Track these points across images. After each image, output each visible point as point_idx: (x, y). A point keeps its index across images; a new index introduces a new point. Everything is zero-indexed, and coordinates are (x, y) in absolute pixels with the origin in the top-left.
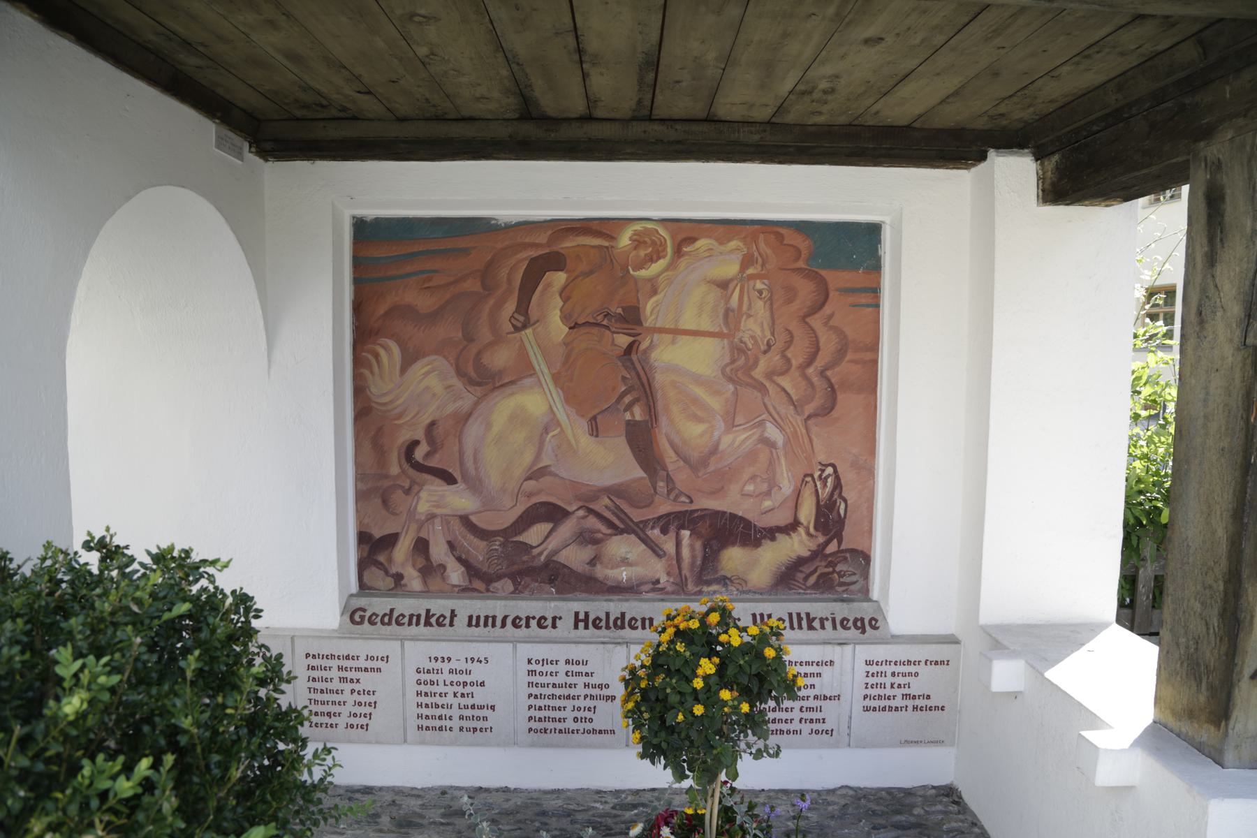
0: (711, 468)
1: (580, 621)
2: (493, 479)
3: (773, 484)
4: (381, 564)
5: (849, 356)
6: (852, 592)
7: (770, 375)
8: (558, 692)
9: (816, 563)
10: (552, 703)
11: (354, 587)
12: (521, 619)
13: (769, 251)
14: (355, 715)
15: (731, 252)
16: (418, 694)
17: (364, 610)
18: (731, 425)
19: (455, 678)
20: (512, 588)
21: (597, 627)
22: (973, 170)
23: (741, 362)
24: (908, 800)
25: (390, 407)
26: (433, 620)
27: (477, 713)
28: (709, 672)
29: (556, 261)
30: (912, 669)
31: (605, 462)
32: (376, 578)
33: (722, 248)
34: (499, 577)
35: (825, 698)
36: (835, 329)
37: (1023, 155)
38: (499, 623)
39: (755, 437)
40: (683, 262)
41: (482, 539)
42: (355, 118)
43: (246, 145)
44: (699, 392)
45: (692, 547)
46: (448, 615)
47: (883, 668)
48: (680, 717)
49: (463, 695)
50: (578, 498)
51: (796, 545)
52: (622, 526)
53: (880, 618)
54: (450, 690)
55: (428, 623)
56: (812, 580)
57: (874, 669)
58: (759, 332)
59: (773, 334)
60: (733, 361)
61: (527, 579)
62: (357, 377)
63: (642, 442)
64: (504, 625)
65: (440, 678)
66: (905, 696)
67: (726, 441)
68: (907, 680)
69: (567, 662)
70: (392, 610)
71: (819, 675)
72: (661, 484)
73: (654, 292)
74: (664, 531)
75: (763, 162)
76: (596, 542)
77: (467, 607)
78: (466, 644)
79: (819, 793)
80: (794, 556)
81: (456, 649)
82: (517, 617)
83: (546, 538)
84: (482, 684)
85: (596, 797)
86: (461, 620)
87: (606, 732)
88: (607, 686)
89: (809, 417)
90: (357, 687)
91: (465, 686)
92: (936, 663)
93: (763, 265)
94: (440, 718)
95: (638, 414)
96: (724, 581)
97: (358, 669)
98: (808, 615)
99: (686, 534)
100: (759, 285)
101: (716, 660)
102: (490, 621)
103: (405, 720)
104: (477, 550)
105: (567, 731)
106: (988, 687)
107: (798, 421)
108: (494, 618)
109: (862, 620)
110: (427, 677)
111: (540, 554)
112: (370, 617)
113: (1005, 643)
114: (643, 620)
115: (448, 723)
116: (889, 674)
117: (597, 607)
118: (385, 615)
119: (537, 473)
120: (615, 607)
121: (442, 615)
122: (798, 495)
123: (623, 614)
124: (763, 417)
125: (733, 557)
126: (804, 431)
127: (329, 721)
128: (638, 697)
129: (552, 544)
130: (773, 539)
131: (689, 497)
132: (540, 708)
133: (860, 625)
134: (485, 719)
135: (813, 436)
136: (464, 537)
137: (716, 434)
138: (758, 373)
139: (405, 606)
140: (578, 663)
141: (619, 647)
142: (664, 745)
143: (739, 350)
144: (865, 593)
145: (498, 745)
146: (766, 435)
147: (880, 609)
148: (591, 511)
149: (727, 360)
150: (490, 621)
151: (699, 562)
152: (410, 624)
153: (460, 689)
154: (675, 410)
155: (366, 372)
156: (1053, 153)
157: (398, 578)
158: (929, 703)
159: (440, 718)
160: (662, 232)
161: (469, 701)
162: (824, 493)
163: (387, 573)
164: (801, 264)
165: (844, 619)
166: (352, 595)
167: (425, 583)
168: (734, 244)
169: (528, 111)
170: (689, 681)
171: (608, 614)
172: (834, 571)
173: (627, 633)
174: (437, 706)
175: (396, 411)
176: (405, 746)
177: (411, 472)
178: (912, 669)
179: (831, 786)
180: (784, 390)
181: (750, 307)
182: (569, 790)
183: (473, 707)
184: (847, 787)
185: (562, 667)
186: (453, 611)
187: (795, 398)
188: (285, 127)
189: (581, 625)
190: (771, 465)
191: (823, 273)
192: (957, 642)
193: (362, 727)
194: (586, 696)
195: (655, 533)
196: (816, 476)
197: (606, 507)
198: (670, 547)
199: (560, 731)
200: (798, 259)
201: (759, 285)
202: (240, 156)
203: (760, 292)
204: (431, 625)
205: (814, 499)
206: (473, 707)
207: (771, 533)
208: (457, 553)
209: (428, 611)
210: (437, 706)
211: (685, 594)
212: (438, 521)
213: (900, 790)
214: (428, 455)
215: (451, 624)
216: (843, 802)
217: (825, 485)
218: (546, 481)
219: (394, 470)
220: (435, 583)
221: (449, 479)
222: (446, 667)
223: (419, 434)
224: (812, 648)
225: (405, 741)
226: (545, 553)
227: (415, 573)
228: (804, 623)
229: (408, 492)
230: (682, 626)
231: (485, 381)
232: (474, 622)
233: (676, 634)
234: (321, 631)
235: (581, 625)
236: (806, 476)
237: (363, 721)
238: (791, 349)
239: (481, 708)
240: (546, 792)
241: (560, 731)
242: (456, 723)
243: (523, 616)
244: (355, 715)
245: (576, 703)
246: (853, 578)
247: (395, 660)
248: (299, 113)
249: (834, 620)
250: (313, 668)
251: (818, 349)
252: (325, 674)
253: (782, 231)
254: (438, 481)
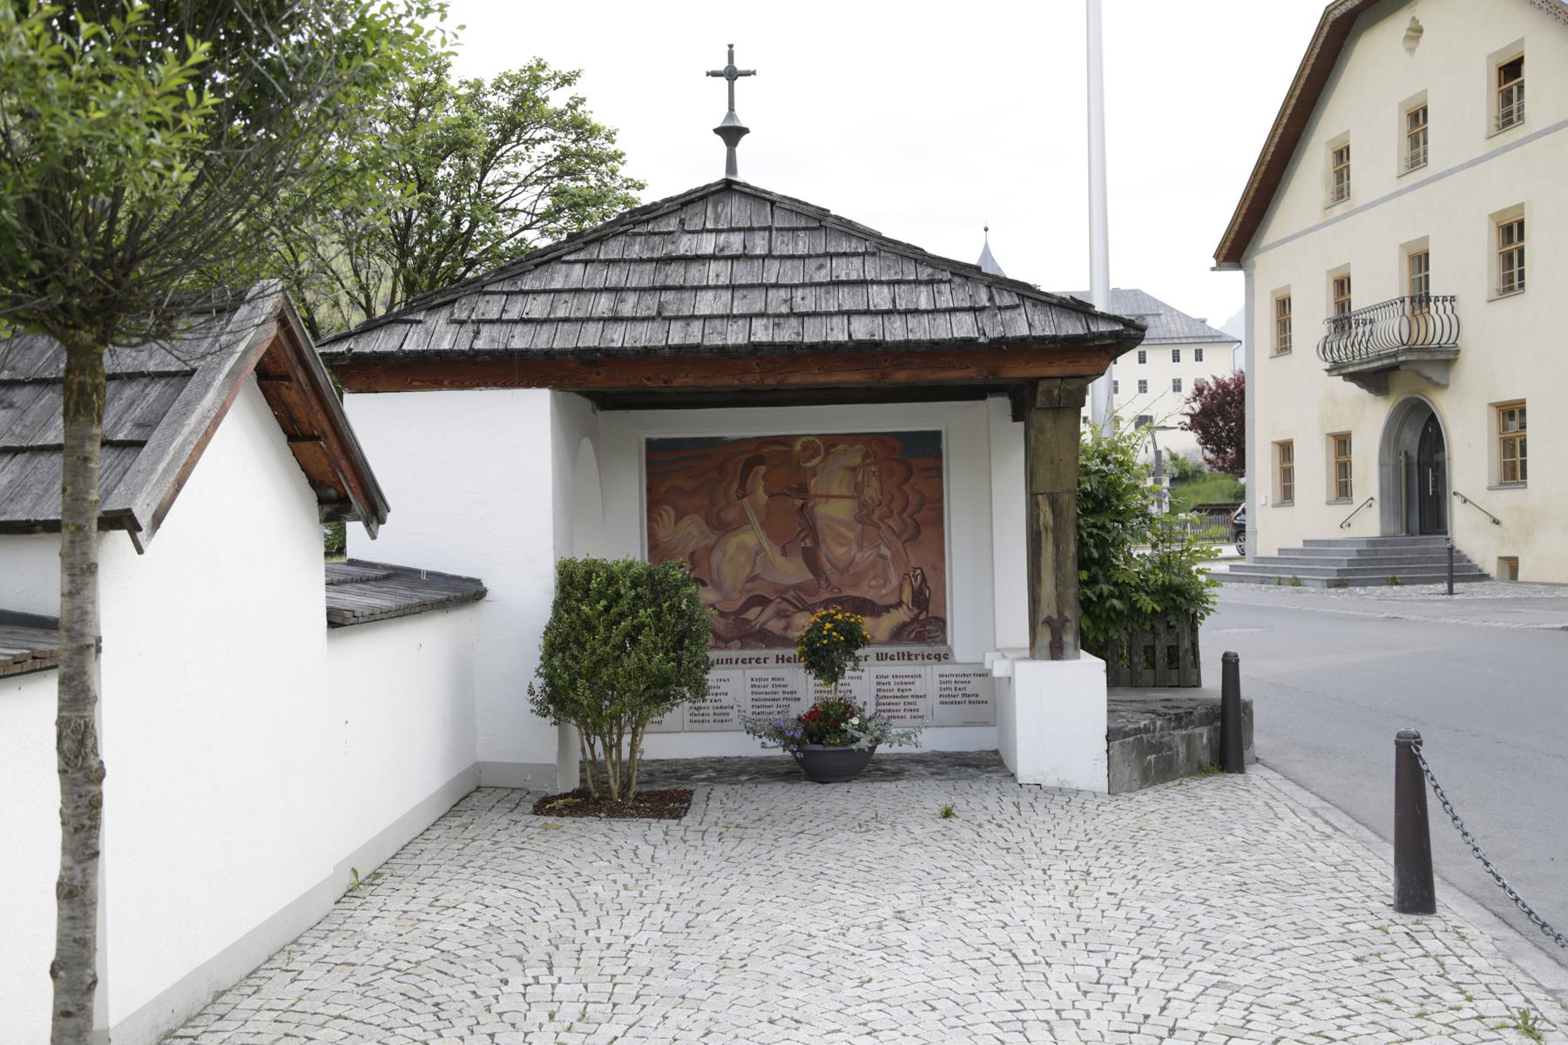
3: (886, 580)
7: (881, 519)
18: (861, 547)
51: (901, 615)
138: (875, 518)
207: (887, 609)
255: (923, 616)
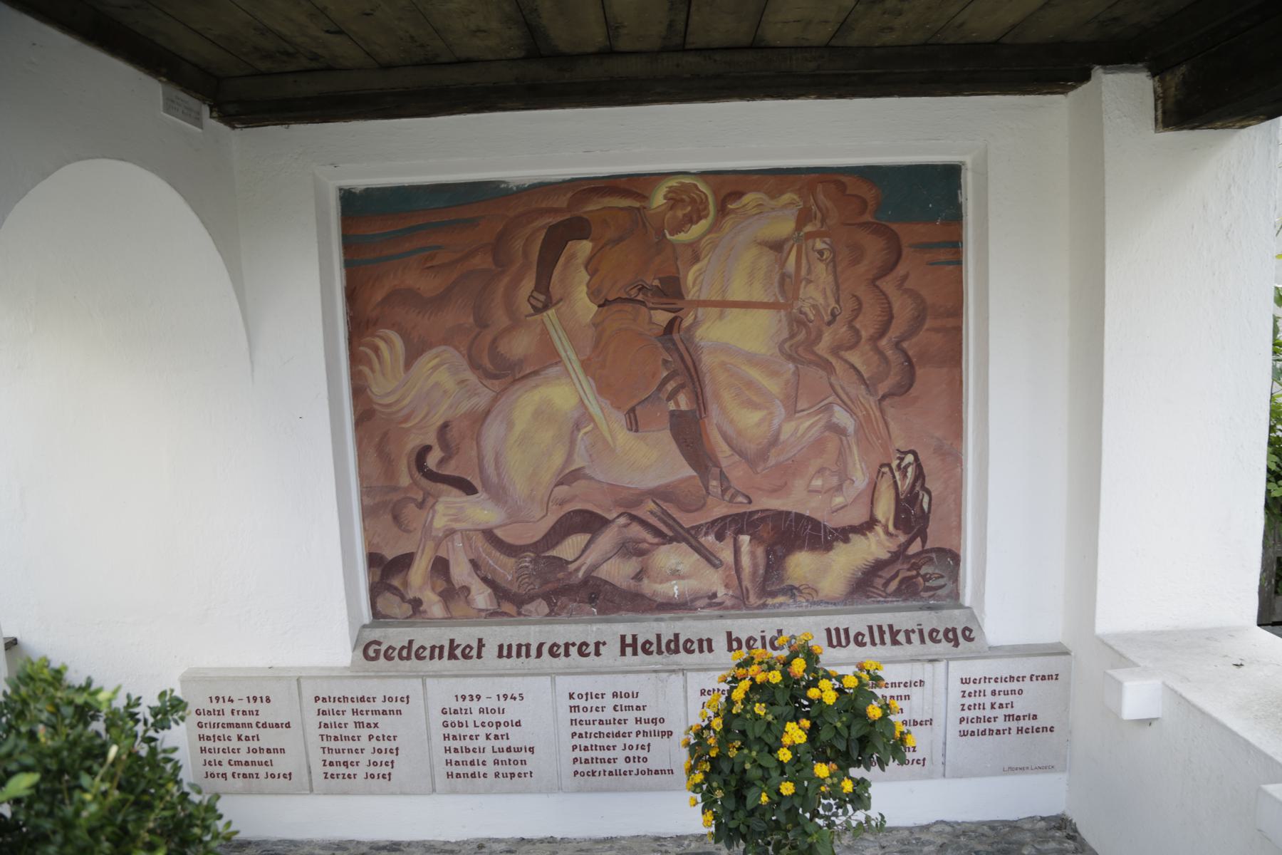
0: (772, 461)
1: (628, 646)
2: (519, 485)
3: (844, 477)
4: (396, 588)
5: (928, 324)
6: (940, 598)
7: (836, 350)
8: (605, 729)
9: (898, 566)
10: (599, 742)
11: (366, 616)
12: (559, 647)
13: (829, 204)
14: (375, 764)
15: (785, 206)
16: (446, 737)
17: (379, 643)
18: (793, 410)
19: (487, 718)
20: (547, 610)
21: (647, 652)
22: (1071, 94)
23: (802, 336)
24: (1016, 837)
25: (395, 409)
26: (458, 652)
27: (513, 756)
28: (798, 741)
29: (577, 228)
30: (1015, 686)
31: (650, 461)
32: (389, 602)
33: (773, 203)
34: (532, 599)
35: (915, 723)
36: (914, 294)
37: (1136, 71)
38: (533, 652)
39: (822, 423)
40: (728, 222)
41: (509, 555)
42: (330, 69)
43: (205, 110)
44: (755, 374)
45: (753, 554)
46: (475, 645)
47: (982, 686)
48: (764, 798)
49: (496, 737)
50: (618, 503)
51: (874, 547)
52: (671, 534)
53: (974, 627)
54: (482, 732)
55: (452, 656)
56: (893, 586)
57: (971, 688)
58: (821, 301)
59: (837, 302)
60: (792, 336)
61: (564, 599)
62: (355, 376)
63: (690, 435)
64: (539, 655)
65: (470, 718)
66: (1008, 717)
67: (788, 429)
68: (1010, 698)
69: (615, 695)
70: (411, 642)
71: (908, 697)
72: (714, 483)
73: (696, 259)
74: (720, 537)
75: (819, 97)
76: (641, 553)
77: (497, 634)
78: (497, 680)
79: (910, 830)
80: (871, 559)
81: (486, 684)
82: (554, 645)
83: (584, 551)
84: (518, 724)
85: (655, 845)
86: (490, 651)
87: (663, 772)
88: (662, 720)
89: (884, 397)
90: (375, 732)
91: (499, 727)
92: (1043, 678)
93: (823, 221)
94: (472, 763)
95: (684, 402)
96: (791, 591)
97: (376, 712)
98: (891, 627)
99: (745, 539)
100: (819, 245)
101: (806, 723)
102: (523, 650)
103: (432, 767)
104: (505, 568)
105: (618, 773)
106: (1117, 716)
107: (871, 403)
108: (528, 646)
109: (954, 630)
110: (456, 718)
111: (578, 570)
112: (386, 651)
113: (1132, 658)
114: (701, 641)
115: (482, 769)
116: (988, 693)
117: (647, 628)
118: (403, 648)
119: (570, 477)
120: (666, 627)
121: (468, 646)
122: (874, 488)
123: (677, 636)
124: (830, 399)
125: (801, 564)
126: (878, 414)
127: (347, 772)
128: (707, 767)
129: (591, 558)
130: (846, 540)
131: (747, 497)
132: (586, 749)
133: (952, 636)
134: (524, 762)
135: (889, 419)
136: (489, 554)
137: (776, 422)
138: (822, 348)
139: (425, 636)
140: (627, 695)
141: (673, 676)
142: (743, 829)
143: (798, 322)
144: (955, 596)
145: (540, 792)
146: (834, 420)
147: (973, 617)
148: (634, 518)
149: (785, 334)
150: (523, 650)
151: (761, 571)
152: (432, 657)
153: (493, 731)
154: (727, 396)
155: (366, 369)
156: (1178, 64)
157: (417, 604)
158: (1036, 724)
159: (472, 763)
160: (702, 187)
161: (504, 744)
162: (904, 485)
163: (403, 598)
164: (867, 218)
165: (933, 630)
166: (364, 626)
167: (447, 608)
168: (787, 197)
169: (537, 47)
170: (772, 751)
171: (659, 637)
172: (918, 574)
173: (682, 657)
174: (468, 750)
175: (401, 414)
176: (435, 796)
177: (425, 482)
178: (1015, 686)
179: (925, 822)
180: (853, 367)
181: (809, 271)
182: (623, 838)
183: (509, 750)
184: (943, 822)
185: (609, 702)
186: (480, 640)
187: (866, 376)
188: (252, 87)
189: (629, 650)
190: (842, 454)
191: (894, 227)
192: (1067, 653)
193: (384, 776)
194: (638, 733)
195: (709, 540)
196: (895, 464)
197: (652, 512)
198: (727, 555)
199: (611, 773)
200: (862, 212)
201: (819, 245)
202: (198, 122)
203: (821, 253)
204: (456, 658)
205: (892, 492)
206: (509, 750)
207: (844, 534)
208: (482, 573)
209: (452, 641)
210: (468, 750)
211: (747, 608)
212: (457, 537)
213: (1005, 823)
214: (442, 462)
215: (479, 656)
216: (939, 841)
217: (905, 476)
218: (580, 485)
219: (405, 481)
220: (458, 607)
221: (469, 489)
222: (475, 706)
223: (431, 439)
224: (899, 667)
225: (434, 790)
226: (584, 569)
227: (435, 598)
228: (887, 637)
229: (421, 505)
230: (759, 679)
231: (505, 373)
232: (505, 653)
233: (751, 688)
234: (332, 669)
235: (629, 650)
236: (882, 466)
237: (385, 770)
238: (860, 318)
239: (518, 750)
240: (597, 841)
241: (611, 773)
242: (490, 769)
243: (561, 643)
244: (375, 764)
245: (628, 741)
246: (941, 582)
247: (417, 700)
248: (264, 66)
249: (921, 632)
250: (324, 713)
251: (891, 317)
252: (338, 719)
253: (843, 179)
254: (455, 491)
255: (915, 547)
